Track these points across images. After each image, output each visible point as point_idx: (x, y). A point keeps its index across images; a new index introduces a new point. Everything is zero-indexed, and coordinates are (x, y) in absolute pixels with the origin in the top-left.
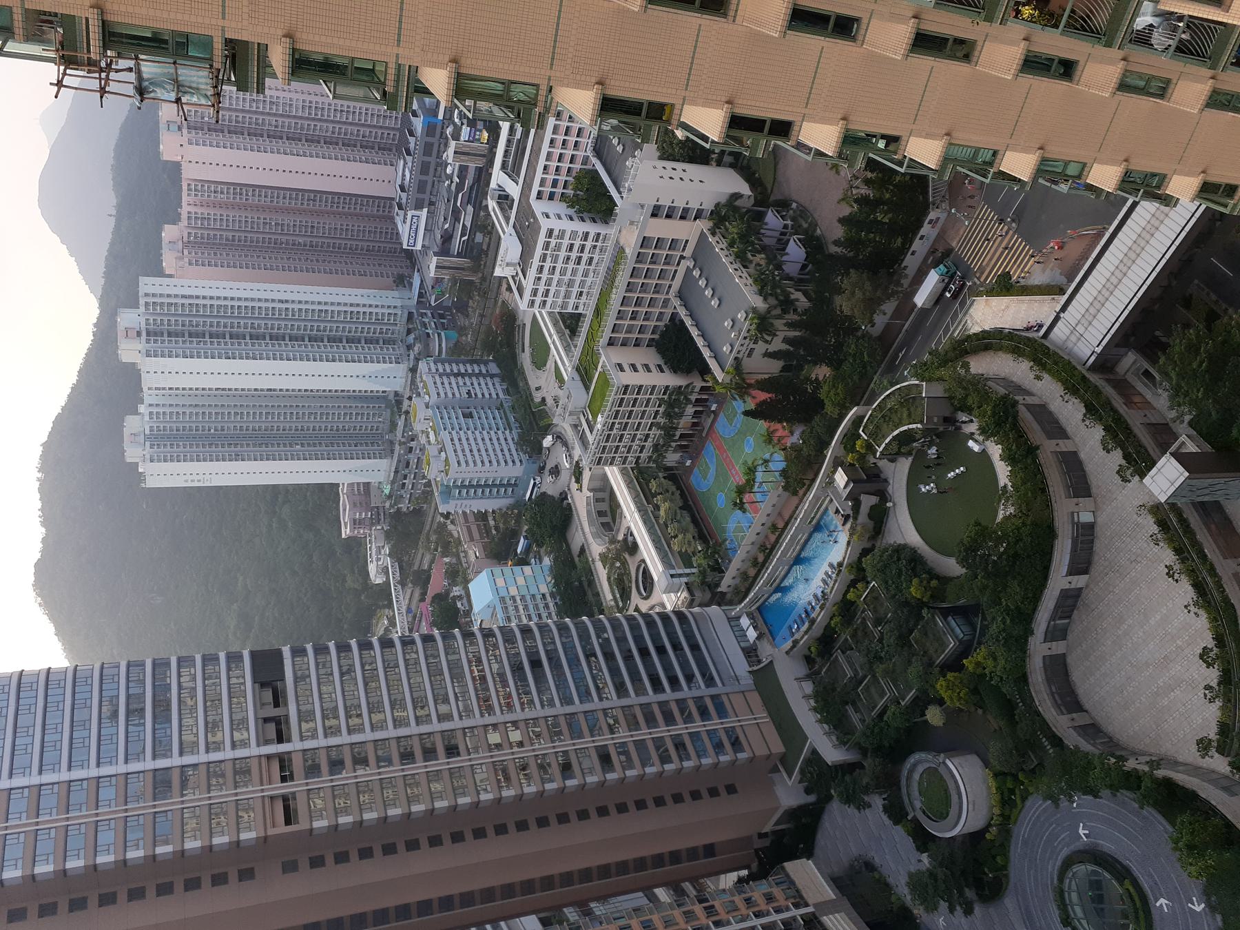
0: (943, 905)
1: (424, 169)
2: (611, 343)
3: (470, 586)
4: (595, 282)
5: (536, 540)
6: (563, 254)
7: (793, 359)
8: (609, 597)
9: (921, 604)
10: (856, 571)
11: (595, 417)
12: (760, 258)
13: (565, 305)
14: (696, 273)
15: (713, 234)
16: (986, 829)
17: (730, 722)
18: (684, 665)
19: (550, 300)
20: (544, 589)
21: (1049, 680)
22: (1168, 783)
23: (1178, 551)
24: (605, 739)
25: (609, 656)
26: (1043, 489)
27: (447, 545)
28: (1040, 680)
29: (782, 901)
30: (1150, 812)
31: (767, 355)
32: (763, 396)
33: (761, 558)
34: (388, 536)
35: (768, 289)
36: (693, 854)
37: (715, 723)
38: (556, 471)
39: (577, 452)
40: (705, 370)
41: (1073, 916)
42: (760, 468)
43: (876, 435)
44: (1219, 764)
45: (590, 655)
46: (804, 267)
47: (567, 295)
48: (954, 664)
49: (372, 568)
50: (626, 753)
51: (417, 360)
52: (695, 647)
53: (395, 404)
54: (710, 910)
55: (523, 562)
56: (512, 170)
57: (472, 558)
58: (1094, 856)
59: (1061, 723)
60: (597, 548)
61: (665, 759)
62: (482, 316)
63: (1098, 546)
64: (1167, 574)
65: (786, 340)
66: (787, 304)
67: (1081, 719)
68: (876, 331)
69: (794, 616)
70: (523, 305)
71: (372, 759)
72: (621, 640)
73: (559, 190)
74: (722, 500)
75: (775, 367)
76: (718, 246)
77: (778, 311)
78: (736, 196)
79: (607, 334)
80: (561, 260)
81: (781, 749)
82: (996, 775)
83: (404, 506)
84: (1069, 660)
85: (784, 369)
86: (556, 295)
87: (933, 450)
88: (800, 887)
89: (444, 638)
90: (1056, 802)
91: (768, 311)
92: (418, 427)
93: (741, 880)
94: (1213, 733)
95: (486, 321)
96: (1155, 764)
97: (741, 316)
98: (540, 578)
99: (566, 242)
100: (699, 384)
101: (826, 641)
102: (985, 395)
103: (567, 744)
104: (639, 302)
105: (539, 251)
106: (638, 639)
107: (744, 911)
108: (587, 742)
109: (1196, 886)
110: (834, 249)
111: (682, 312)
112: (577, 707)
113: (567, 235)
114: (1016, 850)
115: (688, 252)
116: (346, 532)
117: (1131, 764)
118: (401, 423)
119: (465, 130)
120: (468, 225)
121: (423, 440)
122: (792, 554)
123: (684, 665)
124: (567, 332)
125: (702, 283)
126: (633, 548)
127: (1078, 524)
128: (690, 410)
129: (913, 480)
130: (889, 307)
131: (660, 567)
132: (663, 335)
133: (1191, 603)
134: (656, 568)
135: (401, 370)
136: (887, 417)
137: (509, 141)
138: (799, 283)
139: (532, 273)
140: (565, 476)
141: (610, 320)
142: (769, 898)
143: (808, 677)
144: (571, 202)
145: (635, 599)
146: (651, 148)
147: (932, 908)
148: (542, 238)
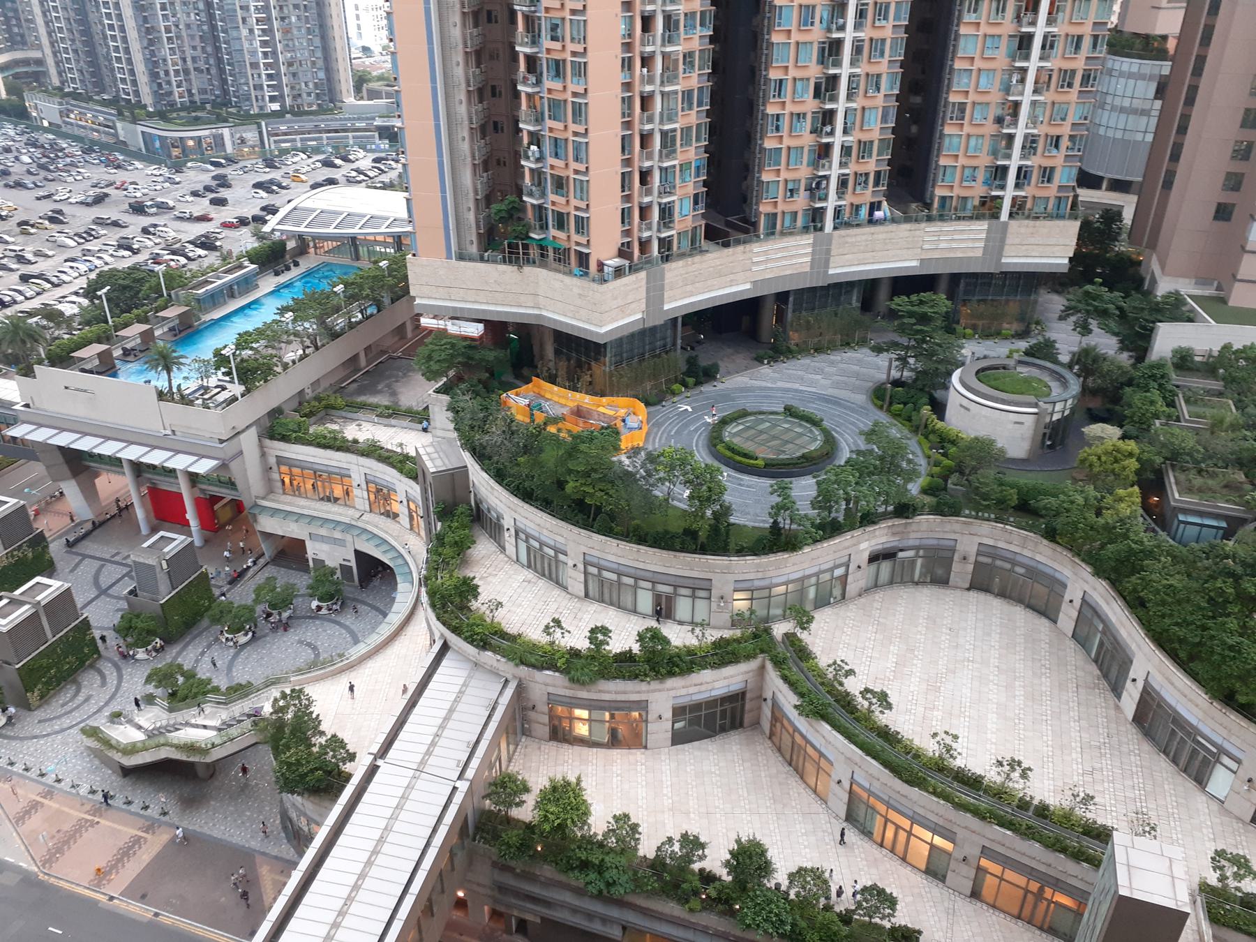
23: (1043, 811)
28: (1038, 558)
41: (789, 419)
63: (1163, 765)
64: (1019, 763)
84: (1044, 622)
88: (1038, 223)
127: (1218, 761)
133: (954, 745)
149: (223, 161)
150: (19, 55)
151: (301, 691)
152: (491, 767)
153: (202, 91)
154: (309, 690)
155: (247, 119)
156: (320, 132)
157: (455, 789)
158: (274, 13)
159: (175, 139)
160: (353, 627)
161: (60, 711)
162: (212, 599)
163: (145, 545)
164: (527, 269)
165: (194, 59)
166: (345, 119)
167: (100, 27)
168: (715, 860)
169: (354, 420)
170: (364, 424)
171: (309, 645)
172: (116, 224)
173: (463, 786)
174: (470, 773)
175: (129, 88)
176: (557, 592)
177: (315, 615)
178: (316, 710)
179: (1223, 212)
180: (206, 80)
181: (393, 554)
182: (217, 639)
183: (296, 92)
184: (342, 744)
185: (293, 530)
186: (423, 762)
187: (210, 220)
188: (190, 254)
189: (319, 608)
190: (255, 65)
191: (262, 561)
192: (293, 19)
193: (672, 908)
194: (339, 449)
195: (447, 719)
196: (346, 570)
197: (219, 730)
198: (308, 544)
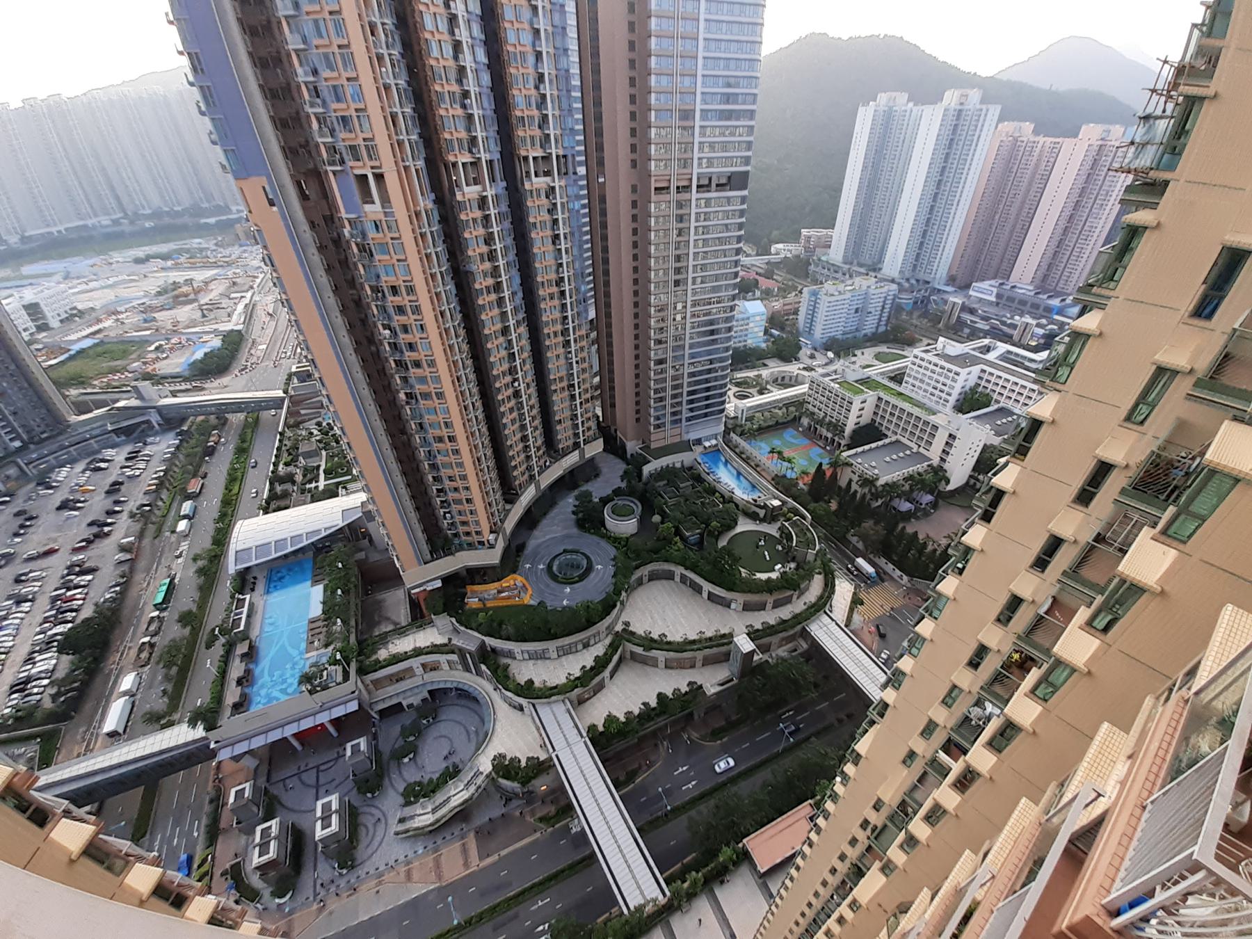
0: (577, 503)
1: (1023, 302)
2: (880, 399)
3: (759, 302)
4: (919, 396)
5: (777, 340)
6: (942, 379)
7: (845, 494)
8: (739, 376)
9: (708, 525)
10: (729, 500)
11: (838, 383)
12: (907, 487)
13: (909, 376)
14: (908, 452)
15: (929, 466)
16: (605, 528)
17: (668, 426)
18: (699, 408)
19: (915, 368)
20: (749, 341)
21: (664, 571)
22: (615, 606)
23: (710, 639)
24: (670, 363)
25: (709, 371)
26: (750, 592)
27: (784, 291)
29: (587, 434)
30: (604, 595)
31: (851, 481)
32: (828, 474)
33: (743, 456)
34: (798, 257)
35: (888, 488)
36: (613, 397)
37: (668, 418)
38: (812, 357)
39: (820, 371)
40: (850, 447)
42: (789, 465)
43: (794, 524)
44: (619, 627)
45: (711, 362)
46: (895, 509)
47: (915, 378)
48: (678, 532)
49: (780, 246)
50: (661, 373)
51: (899, 284)
52: (706, 415)
53: (874, 268)
54: (587, 401)
55: (766, 332)
56: (1005, 357)
57: (774, 304)
58: (589, 569)
59: (645, 571)
60: (765, 373)
61: (656, 391)
62: (916, 326)
65: (856, 492)
66: (876, 496)
67: (645, 579)
68: (849, 537)
69: (712, 466)
70: (916, 351)
71: (679, 239)
72: (716, 379)
73: (983, 383)
74: (777, 443)
75: (843, 483)
76: (921, 467)
77: (873, 490)
78: (948, 482)
79: (886, 397)
80: (939, 378)
81: (653, 446)
82: (627, 538)
83: (812, 268)
85: (840, 487)
86: (918, 372)
87: (780, 548)
89: (735, 284)
90: (613, 560)
91: (875, 486)
92: (857, 280)
93: (598, 417)
94: (631, 628)
95: (912, 328)
96: (622, 603)
97: (876, 471)
98: (755, 340)
99: (949, 382)
100: (843, 442)
101: (698, 479)
102: (803, 578)
103: (671, 343)
104: (900, 418)
105: (947, 365)
106: (715, 388)
107: (585, 416)
108: (670, 354)
109: (573, 604)
110: (901, 526)
111: (887, 441)
112: (687, 351)
113: (953, 384)
114: (595, 538)
115: (921, 450)
116: (804, 232)
117: (624, 594)
118: (863, 270)
119: (1041, 331)
120: (977, 325)
121: (849, 282)
122: (742, 471)
123: (699, 408)
124: (893, 375)
125: (901, 455)
126: (761, 393)
128: (830, 435)
129: (766, 535)
130: (860, 546)
131: (748, 405)
132: (877, 428)
134: (749, 403)
135: (895, 274)
136: (802, 531)
137: (1025, 358)
138: (886, 504)
139: (935, 360)
140: (809, 362)
141: (893, 400)
142: (589, 429)
143: (683, 466)
144: (973, 390)
145: (735, 389)
146: (996, 441)
147: (577, 498)
148: (955, 368)
149: (8, 499)
161: (370, 837)
164: (457, 554)
168: (653, 703)
171: (441, 736)
176: (548, 661)
177: (429, 725)
179: (638, 420)
184: (533, 758)
186: (567, 742)
188: (82, 583)
192: (5, 384)
193: (652, 723)
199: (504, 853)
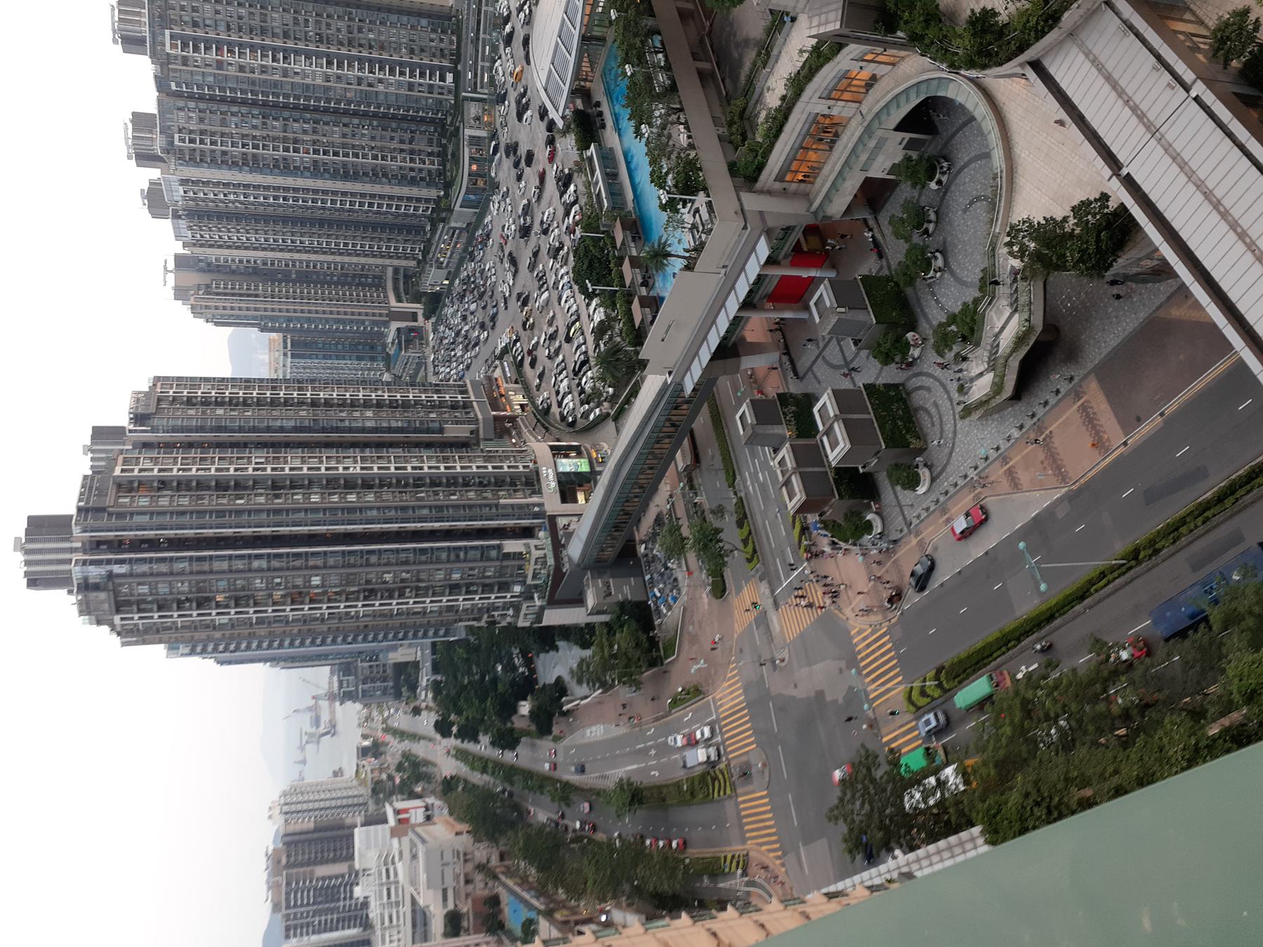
149: (493, 143)
150: (390, 285)
151: (1012, 227)
152: (1196, 49)
153: (430, 142)
154: (1015, 219)
155: (458, 108)
156: (478, 39)
157: (1197, 99)
158: (365, 54)
159: (470, 180)
160: (973, 155)
162: (888, 279)
163: (817, 320)
165: (402, 142)
166: (468, 9)
167: (370, 214)
169: (761, 94)
170: (769, 84)
171: (971, 203)
172: (536, 254)
173: (1199, 89)
174: (1188, 76)
175: (422, 206)
177: (944, 189)
178: (1038, 218)
180: (422, 136)
181: (913, 94)
182: (930, 286)
183: (438, 53)
184: (1085, 204)
185: (852, 185)
187: (544, 170)
188: (572, 199)
189: (939, 182)
190: (411, 87)
191: (871, 223)
192: (371, 36)
194: (786, 118)
195: (1115, 86)
196: (910, 145)
197: (1016, 310)
198: (872, 174)
199: (1171, 407)
